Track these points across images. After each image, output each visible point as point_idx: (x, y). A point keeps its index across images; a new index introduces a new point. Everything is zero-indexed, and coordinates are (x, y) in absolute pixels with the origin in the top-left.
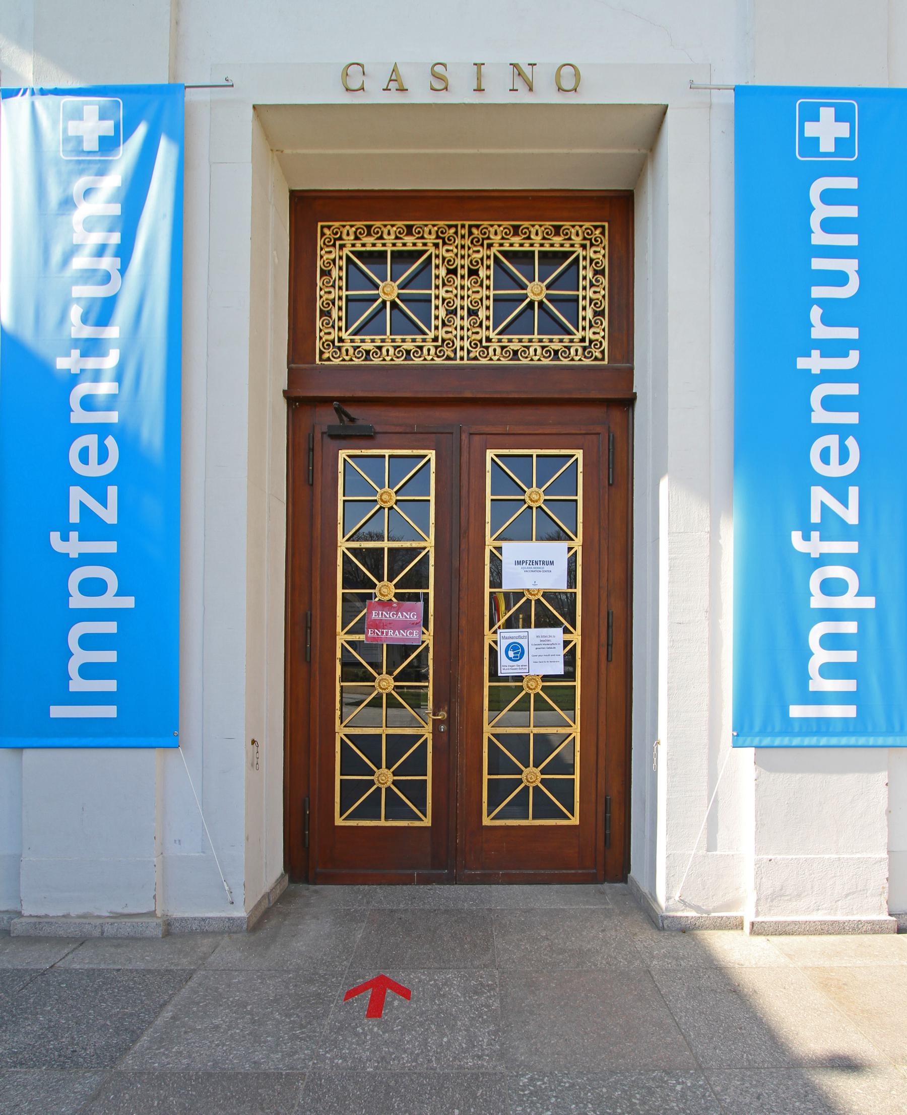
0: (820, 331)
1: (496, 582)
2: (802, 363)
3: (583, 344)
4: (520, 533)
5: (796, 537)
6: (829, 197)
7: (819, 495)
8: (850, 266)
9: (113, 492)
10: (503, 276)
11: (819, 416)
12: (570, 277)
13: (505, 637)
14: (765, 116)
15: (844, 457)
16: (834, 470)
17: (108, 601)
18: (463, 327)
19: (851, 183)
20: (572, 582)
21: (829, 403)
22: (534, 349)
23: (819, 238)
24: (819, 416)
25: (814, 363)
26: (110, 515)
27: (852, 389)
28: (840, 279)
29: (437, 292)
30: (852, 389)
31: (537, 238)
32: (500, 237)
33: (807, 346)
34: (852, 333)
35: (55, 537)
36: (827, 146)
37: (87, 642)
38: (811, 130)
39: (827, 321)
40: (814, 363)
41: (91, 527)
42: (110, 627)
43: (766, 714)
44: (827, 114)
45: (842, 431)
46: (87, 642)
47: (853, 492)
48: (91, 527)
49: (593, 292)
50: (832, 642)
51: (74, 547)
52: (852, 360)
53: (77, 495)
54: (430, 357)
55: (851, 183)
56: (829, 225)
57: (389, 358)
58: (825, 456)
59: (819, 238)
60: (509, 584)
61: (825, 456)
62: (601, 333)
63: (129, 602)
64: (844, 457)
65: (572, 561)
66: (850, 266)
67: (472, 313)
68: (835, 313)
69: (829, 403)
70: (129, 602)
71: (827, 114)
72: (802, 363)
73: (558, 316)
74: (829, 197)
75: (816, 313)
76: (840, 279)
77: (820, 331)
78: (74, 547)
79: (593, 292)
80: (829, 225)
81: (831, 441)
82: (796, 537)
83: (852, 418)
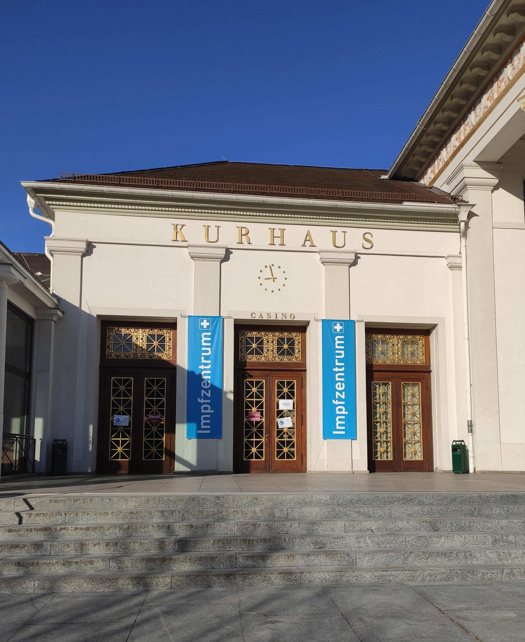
0: (337, 364)
1: (278, 407)
2: (334, 370)
4: (283, 397)
5: (333, 401)
6: (339, 340)
7: (337, 393)
8: (343, 352)
9: (209, 391)
10: (279, 343)
11: (337, 379)
13: (279, 420)
14: (328, 324)
15: (342, 386)
16: (340, 389)
17: (209, 411)
19: (343, 337)
20: (294, 408)
21: (339, 377)
23: (337, 347)
24: (337, 379)
25: (336, 369)
26: (209, 395)
27: (343, 374)
28: (341, 354)
29: (265, 346)
30: (343, 374)
33: (335, 366)
34: (343, 364)
35: (199, 399)
36: (338, 330)
37: (205, 419)
38: (335, 327)
39: (338, 362)
40: (336, 369)
41: (205, 397)
42: (209, 416)
43: (328, 434)
44: (338, 324)
45: (341, 382)
46: (205, 419)
47: (344, 393)
48: (205, 397)
50: (340, 420)
51: (202, 401)
52: (343, 369)
53: (203, 391)
54: (263, 359)
55: (343, 337)
56: (339, 345)
58: (338, 386)
59: (337, 347)
60: (280, 409)
61: (338, 386)
63: (212, 411)
64: (342, 386)
65: (294, 404)
66: (343, 352)
67: (272, 351)
68: (340, 360)
69: (339, 377)
70: (212, 411)
71: (338, 324)
72: (334, 370)
74: (339, 340)
75: (336, 360)
76: (341, 354)
77: (337, 364)
78: (202, 401)
80: (339, 345)
81: (339, 384)
82: (333, 401)
83: (343, 379)
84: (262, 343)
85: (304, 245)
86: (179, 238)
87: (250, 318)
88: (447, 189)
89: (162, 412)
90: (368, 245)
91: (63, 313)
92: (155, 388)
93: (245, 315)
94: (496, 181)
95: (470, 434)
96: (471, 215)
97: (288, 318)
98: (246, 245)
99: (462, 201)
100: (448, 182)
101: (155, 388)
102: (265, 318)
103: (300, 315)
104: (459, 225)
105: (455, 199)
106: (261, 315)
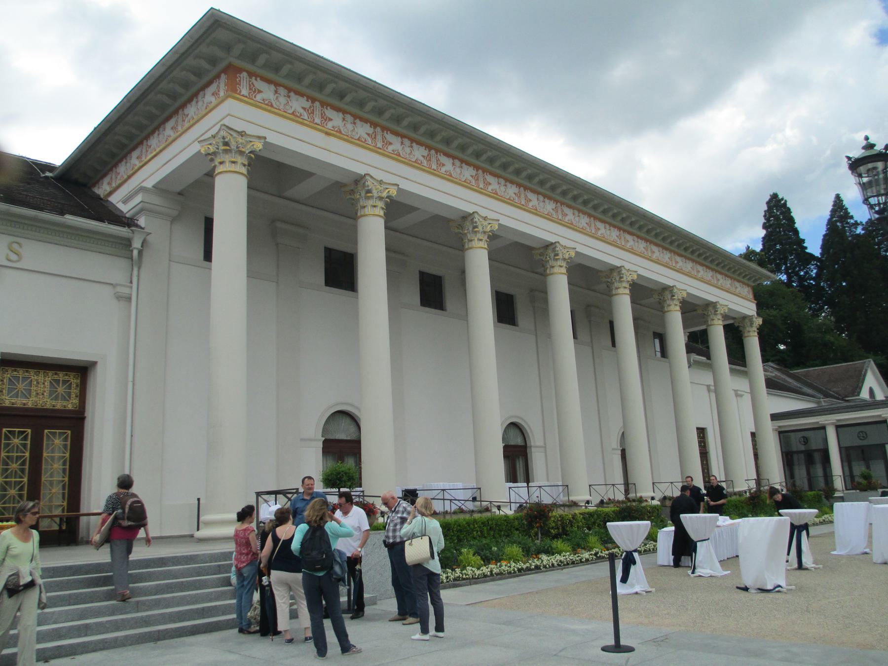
94: (175, 213)
96: (144, 243)
99: (137, 226)
104: (132, 251)
105: (129, 222)
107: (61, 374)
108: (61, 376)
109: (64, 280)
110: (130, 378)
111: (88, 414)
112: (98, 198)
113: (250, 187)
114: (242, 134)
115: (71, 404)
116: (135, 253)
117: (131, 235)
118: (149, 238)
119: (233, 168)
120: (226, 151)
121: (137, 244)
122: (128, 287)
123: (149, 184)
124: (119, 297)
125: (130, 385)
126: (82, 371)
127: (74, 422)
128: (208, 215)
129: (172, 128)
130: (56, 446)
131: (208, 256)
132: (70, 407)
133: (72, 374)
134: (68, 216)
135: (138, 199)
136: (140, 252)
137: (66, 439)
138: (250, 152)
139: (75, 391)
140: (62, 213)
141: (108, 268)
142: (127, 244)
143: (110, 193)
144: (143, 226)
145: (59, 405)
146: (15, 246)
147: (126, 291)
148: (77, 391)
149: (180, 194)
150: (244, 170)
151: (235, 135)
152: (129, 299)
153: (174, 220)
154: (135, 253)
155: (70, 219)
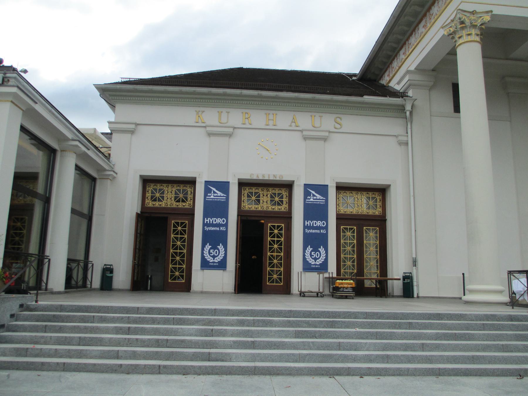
3: (284, 208)
10: (272, 197)
12: (282, 197)
18: (265, 204)
22: (277, 208)
29: (261, 199)
31: (277, 191)
32: (271, 191)
49: (285, 200)
54: (260, 209)
57: (253, 209)
62: (287, 206)
73: (280, 203)
79: (285, 200)
84: (259, 196)
85: (291, 126)
86: (200, 121)
87: (249, 177)
88: (398, 88)
89: (184, 246)
90: (338, 126)
91: (117, 174)
92: (179, 228)
93: (247, 175)
95: (414, 268)
97: (278, 179)
98: (248, 126)
99: (407, 96)
100: (398, 83)
101: (179, 228)
102: (261, 178)
103: (286, 177)
104: (406, 113)
105: (402, 95)
106: (258, 176)
107: (370, 193)
108: (371, 194)
109: (368, 136)
110: (412, 194)
111: (388, 217)
112: (383, 86)
113: (485, 56)
114: (473, 13)
115: (378, 212)
116: (408, 113)
117: (404, 102)
118: (415, 103)
119: (469, 38)
120: (462, 28)
121: (408, 107)
122: (406, 136)
123: (412, 68)
124: (400, 143)
125: (412, 198)
126: (382, 191)
127: (380, 222)
128: (455, 82)
129: (423, 27)
130: (371, 237)
131: (457, 109)
132: (377, 213)
133: (377, 193)
134: (365, 97)
135: (407, 79)
136: (411, 113)
137: (376, 233)
138: (482, 25)
139: (379, 204)
140: (362, 96)
141: (391, 126)
142: (402, 108)
143: (390, 81)
144: (411, 96)
145: (371, 212)
146: (338, 120)
147: (405, 139)
148: (380, 203)
149: (433, 70)
150: (478, 39)
151: (468, 15)
152: (407, 144)
153: (431, 88)
154: (408, 113)
155: (367, 98)
